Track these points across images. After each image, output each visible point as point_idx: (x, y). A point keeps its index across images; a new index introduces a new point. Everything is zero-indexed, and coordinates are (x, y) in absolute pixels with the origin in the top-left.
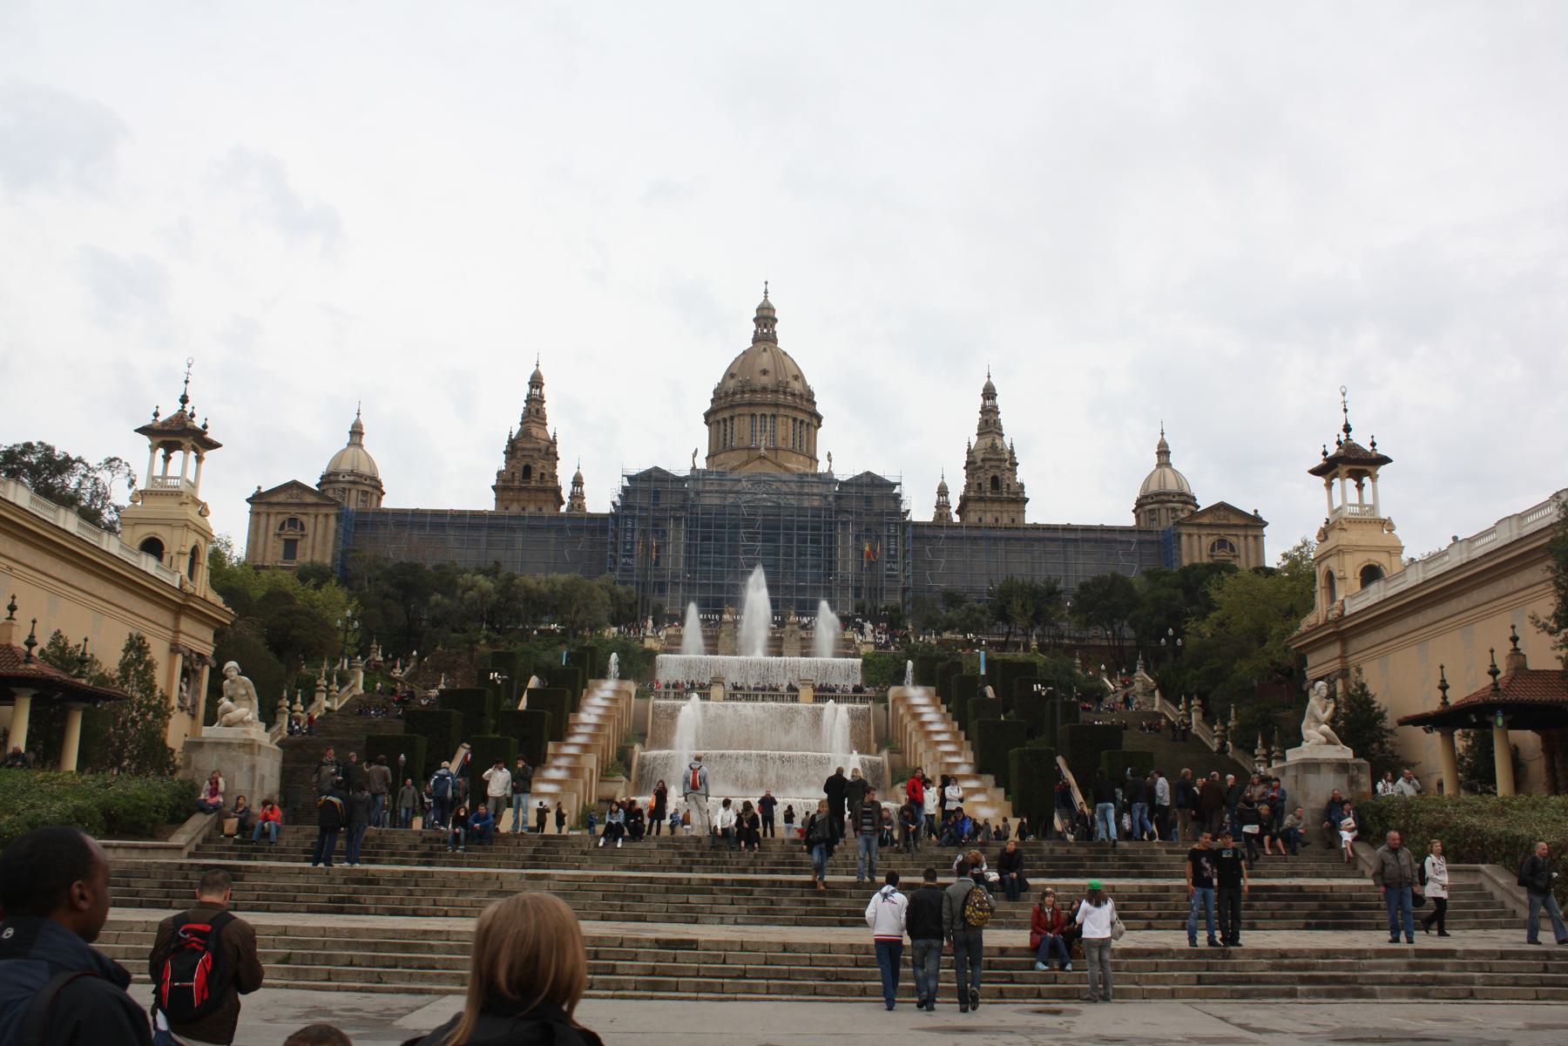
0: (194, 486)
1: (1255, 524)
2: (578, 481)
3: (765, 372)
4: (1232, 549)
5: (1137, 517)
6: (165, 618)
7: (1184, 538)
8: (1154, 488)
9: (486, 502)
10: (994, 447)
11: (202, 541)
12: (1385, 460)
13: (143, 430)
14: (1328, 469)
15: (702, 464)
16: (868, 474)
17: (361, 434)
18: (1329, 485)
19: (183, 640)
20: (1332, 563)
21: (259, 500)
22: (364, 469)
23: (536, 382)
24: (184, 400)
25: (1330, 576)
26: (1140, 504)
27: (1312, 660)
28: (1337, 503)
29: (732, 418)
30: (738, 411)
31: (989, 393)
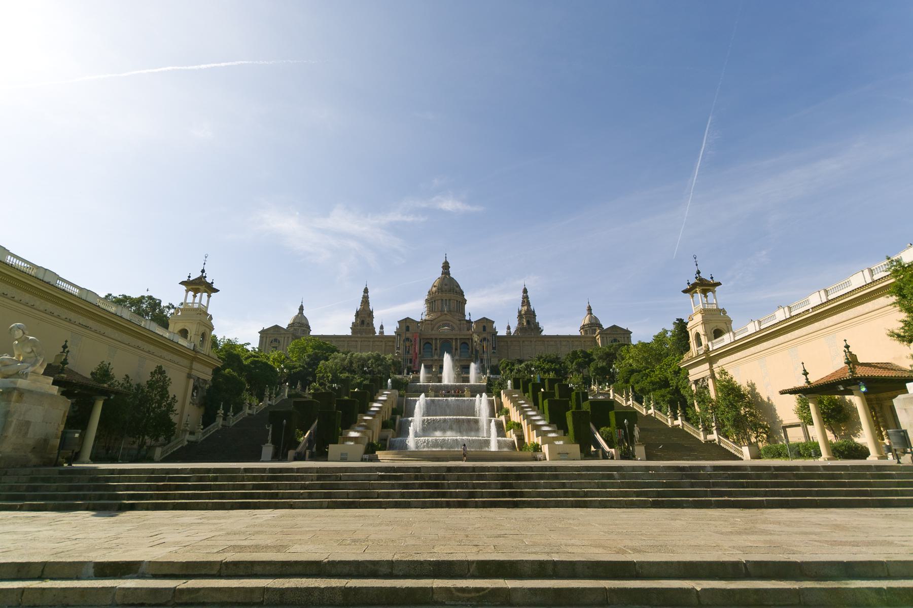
0: (207, 308)
2: (382, 327)
6: (186, 362)
9: (349, 332)
11: (208, 330)
12: (719, 284)
13: (183, 283)
14: (690, 290)
15: (424, 318)
19: (194, 373)
21: (263, 333)
22: (304, 321)
23: (366, 291)
24: (203, 271)
27: (691, 372)
31: (525, 291)
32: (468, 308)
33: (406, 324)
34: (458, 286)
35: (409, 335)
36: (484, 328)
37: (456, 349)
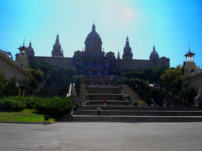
1: (168, 60)
3: (94, 36)
4: (165, 63)
5: (150, 58)
7: (158, 62)
8: (152, 54)
9: (50, 55)
10: (128, 47)
12: (194, 54)
14: (187, 56)
16: (111, 52)
17: (31, 44)
18: (187, 58)
20: (187, 69)
22: (32, 50)
24: (24, 44)
25: (187, 70)
26: (150, 56)
28: (188, 60)
29: (89, 43)
30: (90, 42)
31: (127, 39)
32: (103, 46)
33: (77, 53)
34: (99, 36)
35: (79, 58)
36: (110, 55)
37: (98, 64)
